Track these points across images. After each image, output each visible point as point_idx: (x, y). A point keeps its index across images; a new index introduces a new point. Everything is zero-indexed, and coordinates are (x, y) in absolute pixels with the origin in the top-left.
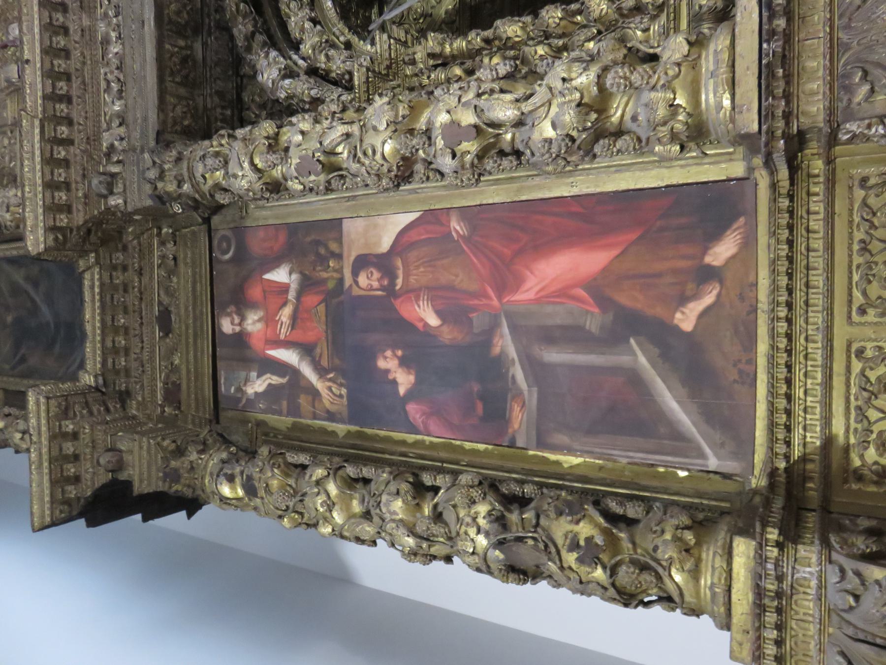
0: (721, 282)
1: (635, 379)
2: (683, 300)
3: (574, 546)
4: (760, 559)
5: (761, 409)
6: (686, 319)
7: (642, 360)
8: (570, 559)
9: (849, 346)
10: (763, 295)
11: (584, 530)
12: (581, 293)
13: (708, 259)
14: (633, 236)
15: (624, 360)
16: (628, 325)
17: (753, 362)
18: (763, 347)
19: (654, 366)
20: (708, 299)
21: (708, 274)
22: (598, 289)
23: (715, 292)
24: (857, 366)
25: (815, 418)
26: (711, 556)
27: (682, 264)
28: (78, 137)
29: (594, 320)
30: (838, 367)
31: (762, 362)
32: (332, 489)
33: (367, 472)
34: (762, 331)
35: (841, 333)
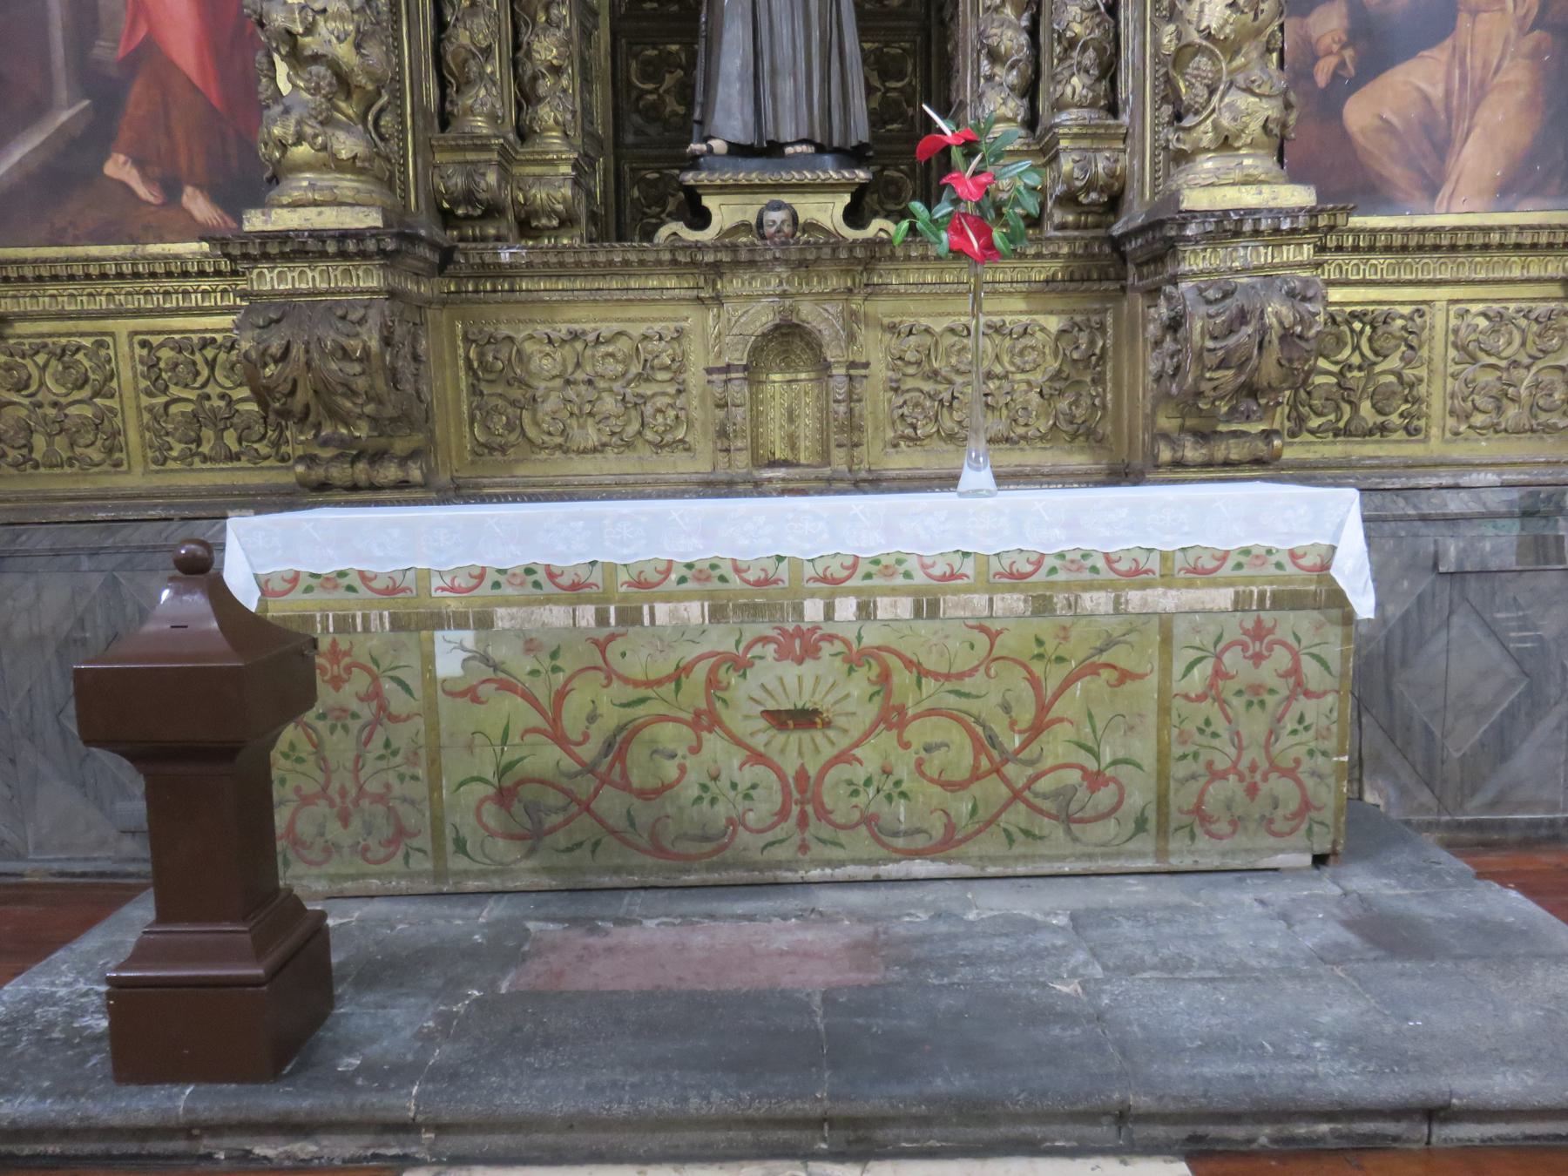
0: (163, 204)
1: (39, 108)
2: (140, 164)
5: (28, 253)
6: (118, 167)
7: (64, 116)
9: (112, 334)
10: (155, 249)
12: (142, 32)
13: (189, 190)
14: (215, 100)
15: (62, 94)
16: (105, 94)
17: (76, 242)
18: (95, 251)
19: (59, 130)
20: (142, 191)
21: (171, 190)
22: (148, 55)
23: (151, 199)
24: (87, 342)
25: (27, 305)
27: (183, 161)
29: (108, 51)
30: (85, 325)
31: (79, 251)
34: (114, 250)
35: (122, 326)
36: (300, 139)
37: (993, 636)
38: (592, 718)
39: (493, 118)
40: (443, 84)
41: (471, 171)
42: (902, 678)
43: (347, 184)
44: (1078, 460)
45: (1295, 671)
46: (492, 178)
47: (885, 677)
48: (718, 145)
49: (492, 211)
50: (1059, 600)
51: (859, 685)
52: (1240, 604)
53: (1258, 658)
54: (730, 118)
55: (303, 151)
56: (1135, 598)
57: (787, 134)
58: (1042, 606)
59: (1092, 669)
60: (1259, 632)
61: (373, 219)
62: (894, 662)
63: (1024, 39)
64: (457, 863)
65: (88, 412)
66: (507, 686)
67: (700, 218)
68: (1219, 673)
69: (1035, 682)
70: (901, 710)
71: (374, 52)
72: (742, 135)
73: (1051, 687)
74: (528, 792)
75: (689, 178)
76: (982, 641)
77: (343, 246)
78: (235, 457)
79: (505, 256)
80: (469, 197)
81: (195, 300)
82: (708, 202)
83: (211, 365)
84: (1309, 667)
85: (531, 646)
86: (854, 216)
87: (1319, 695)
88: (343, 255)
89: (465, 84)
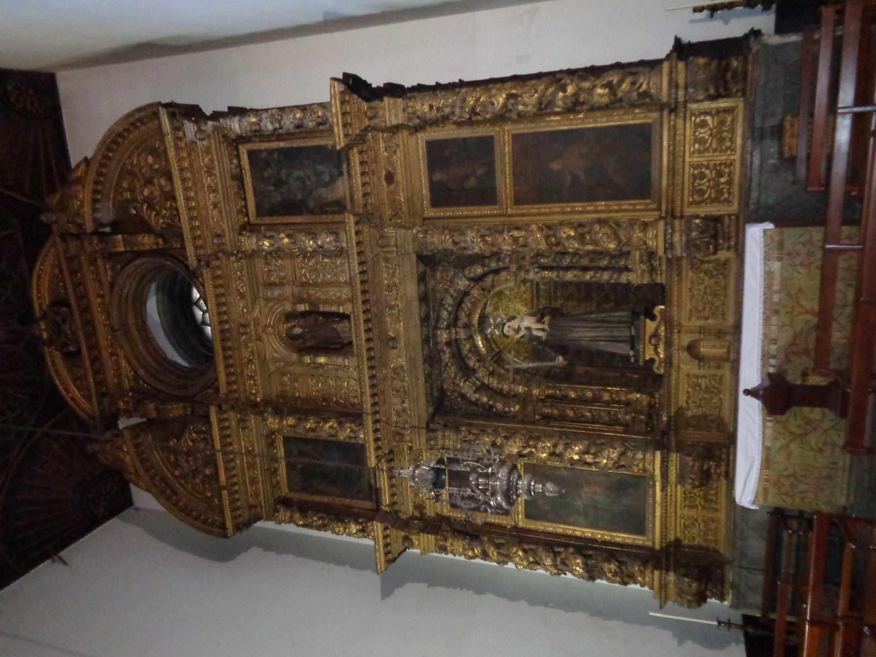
3: (610, 572)
4: (660, 578)
8: (610, 575)
11: (613, 567)
26: (648, 573)
28: (384, 419)
30: (678, 520)
32: (520, 553)
33: (532, 547)
36: (638, 466)
37: (784, 325)
38: (799, 426)
39: (626, 414)
40: (617, 424)
41: (641, 421)
42: (795, 349)
43: (648, 456)
44: (734, 267)
45: (803, 243)
46: (642, 417)
47: (793, 353)
48: (631, 353)
49: (650, 417)
50: (775, 307)
51: (796, 360)
52: (780, 259)
53: (798, 254)
54: (623, 349)
55: (641, 465)
56: (776, 288)
57: (628, 334)
58: (776, 312)
59: (797, 300)
60: (789, 254)
61: (658, 454)
62: (789, 350)
63: (605, 273)
64: (840, 464)
65: (702, 524)
66: (787, 446)
67: (652, 361)
68: (802, 264)
69: (800, 314)
70: (804, 349)
71: (616, 445)
72: (629, 347)
73: (800, 309)
74: (820, 445)
75: (641, 364)
76: (785, 328)
77: (665, 461)
78: (717, 493)
79: (665, 419)
80: (647, 424)
81: (673, 493)
82: (647, 358)
83: (691, 493)
84: (803, 239)
85: (775, 439)
86: (653, 318)
87: (811, 238)
88: (667, 462)
89: (618, 419)
